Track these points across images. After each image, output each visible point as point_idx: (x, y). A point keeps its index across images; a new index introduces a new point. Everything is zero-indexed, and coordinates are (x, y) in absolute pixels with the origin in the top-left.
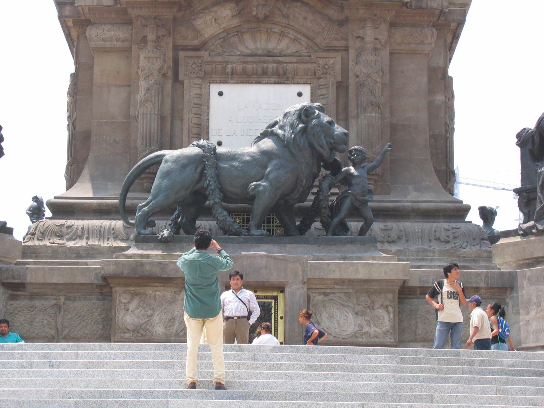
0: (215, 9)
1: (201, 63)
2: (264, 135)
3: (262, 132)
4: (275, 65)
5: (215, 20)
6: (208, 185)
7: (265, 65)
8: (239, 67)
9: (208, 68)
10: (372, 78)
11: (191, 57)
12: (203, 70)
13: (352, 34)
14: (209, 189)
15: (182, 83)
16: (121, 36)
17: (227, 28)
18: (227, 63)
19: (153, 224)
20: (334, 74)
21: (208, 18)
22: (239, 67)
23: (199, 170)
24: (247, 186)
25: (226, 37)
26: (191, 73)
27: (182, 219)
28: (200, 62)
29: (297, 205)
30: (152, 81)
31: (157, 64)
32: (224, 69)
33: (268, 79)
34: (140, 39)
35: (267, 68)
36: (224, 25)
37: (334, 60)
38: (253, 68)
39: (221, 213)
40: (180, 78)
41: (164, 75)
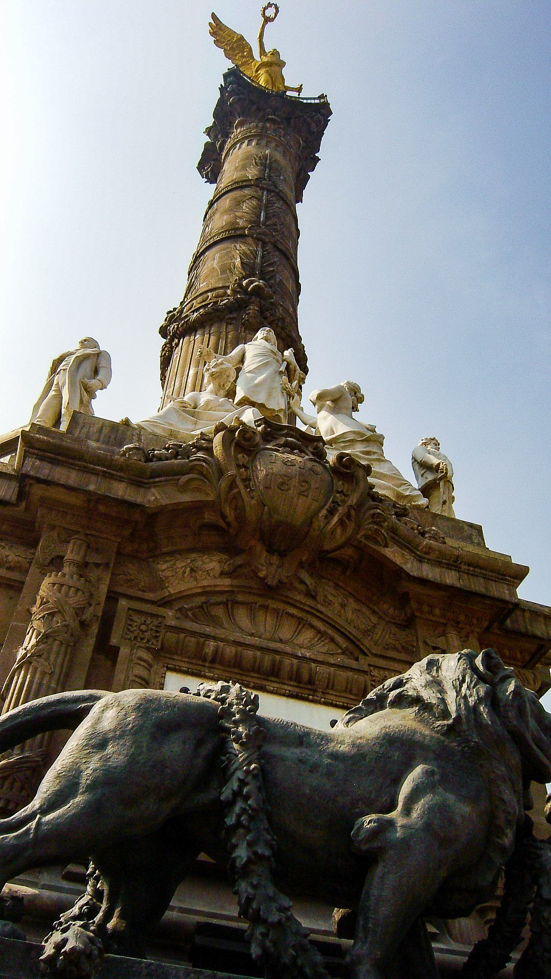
0: (193, 555)
4: (295, 661)
5: (192, 570)
6: (237, 794)
7: (278, 657)
8: (230, 651)
9: (171, 637)
11: (140, 612)
13: (425, 643)
14: (237, 809)
15: (115, 651)
16: (10, 558)
17: (208, 589)
18: (208, 637)
21: (180, 564)
22: (230, 651)
23: (205, 750)
24: (348, 820)
25: (205, 605)
26: (135, 638)
27: (108, 916)
30: (58, 622)
31: (75, 600)
32: (200, 647)
33: (276, 685)
34: (50, 558)
35: (281, 662)
36: (205, 583)
38: (255, 657)
39: (272, 899)
40: (114, 641)
41: (83, 625)
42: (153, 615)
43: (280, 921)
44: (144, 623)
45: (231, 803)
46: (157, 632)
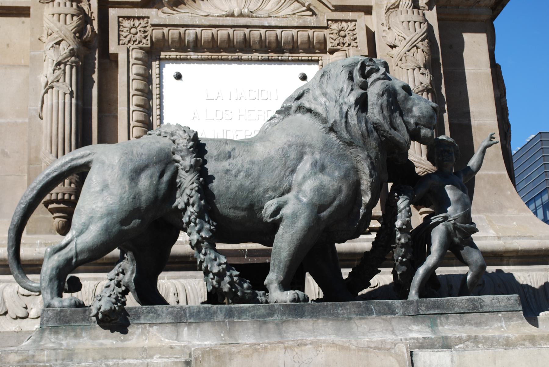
1: (146, 27)
2: (285, 111)
3: (279, 108)
6: (187, 204)
10: (418, 48)
11: (128, 18)
12: (149, 38)
19: (76, 286)
20: (355, 45)
26: (129, 42)
28: (143, 24)
29: (339, 247)
30: (64, 49)
37: (354, 23)
40: (113, 48)
42: (139, 18)
43: (219, 271)
44: (134, 27)
45: (184, 210)
46: (145, 32)
